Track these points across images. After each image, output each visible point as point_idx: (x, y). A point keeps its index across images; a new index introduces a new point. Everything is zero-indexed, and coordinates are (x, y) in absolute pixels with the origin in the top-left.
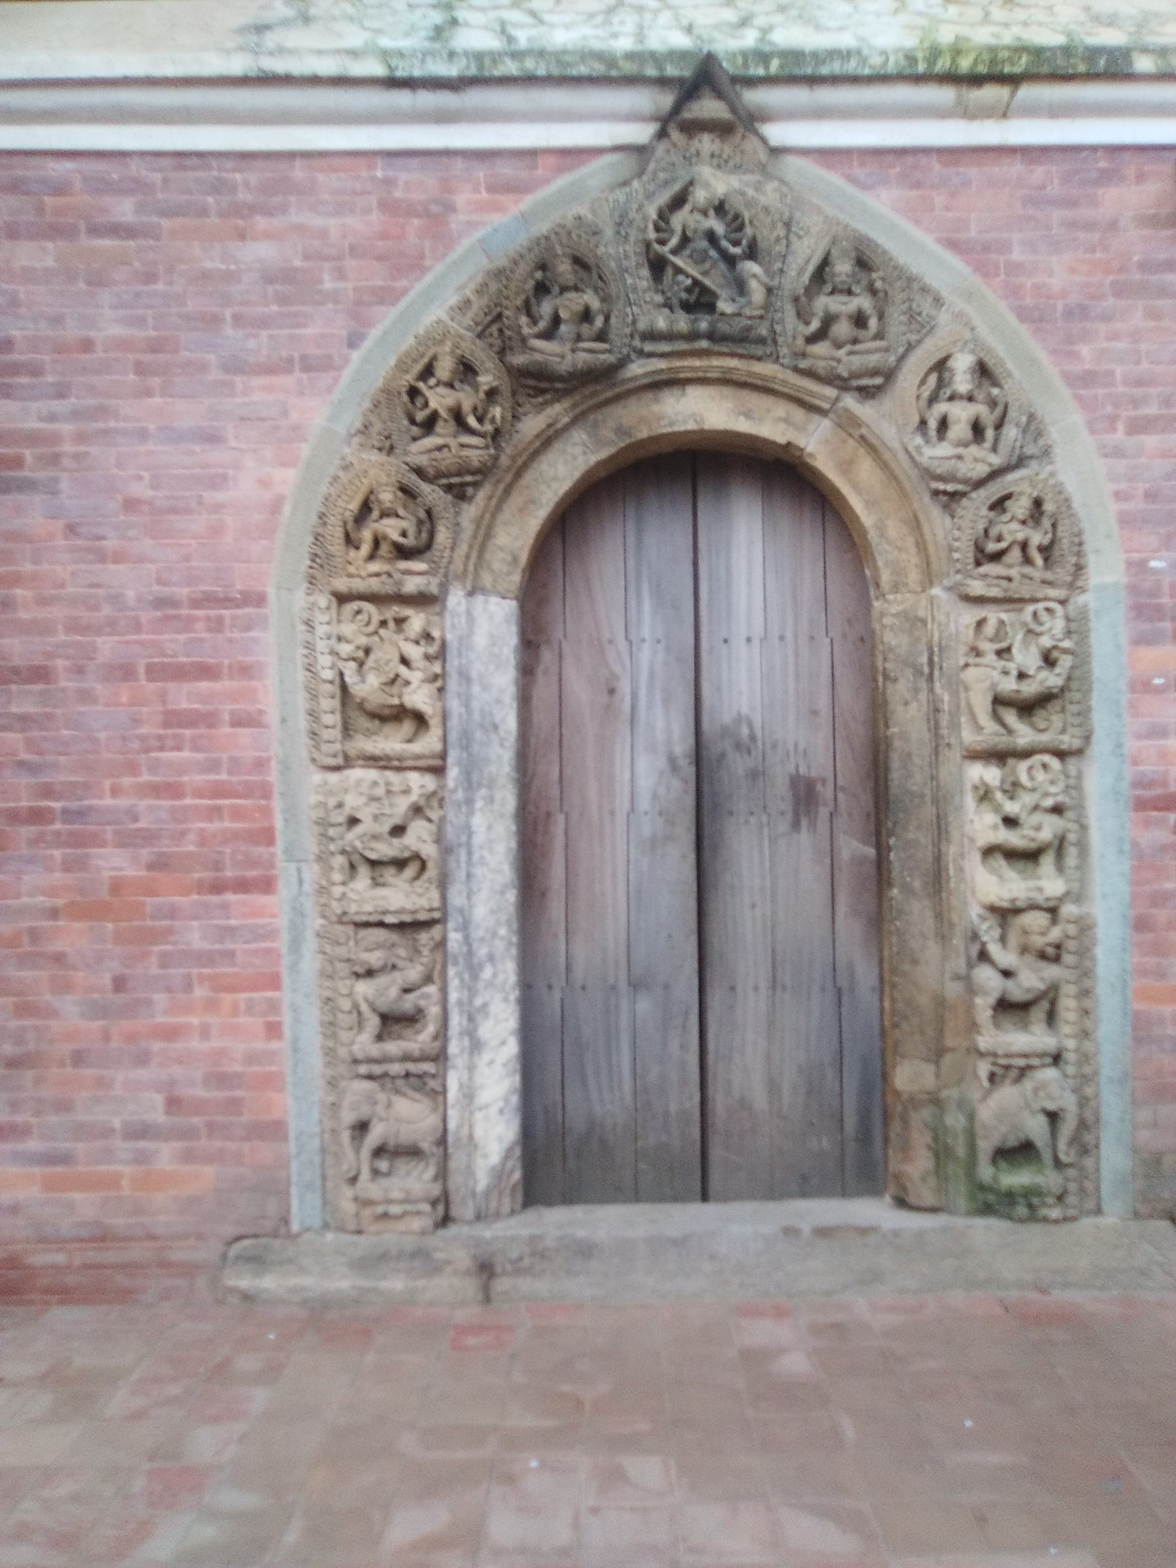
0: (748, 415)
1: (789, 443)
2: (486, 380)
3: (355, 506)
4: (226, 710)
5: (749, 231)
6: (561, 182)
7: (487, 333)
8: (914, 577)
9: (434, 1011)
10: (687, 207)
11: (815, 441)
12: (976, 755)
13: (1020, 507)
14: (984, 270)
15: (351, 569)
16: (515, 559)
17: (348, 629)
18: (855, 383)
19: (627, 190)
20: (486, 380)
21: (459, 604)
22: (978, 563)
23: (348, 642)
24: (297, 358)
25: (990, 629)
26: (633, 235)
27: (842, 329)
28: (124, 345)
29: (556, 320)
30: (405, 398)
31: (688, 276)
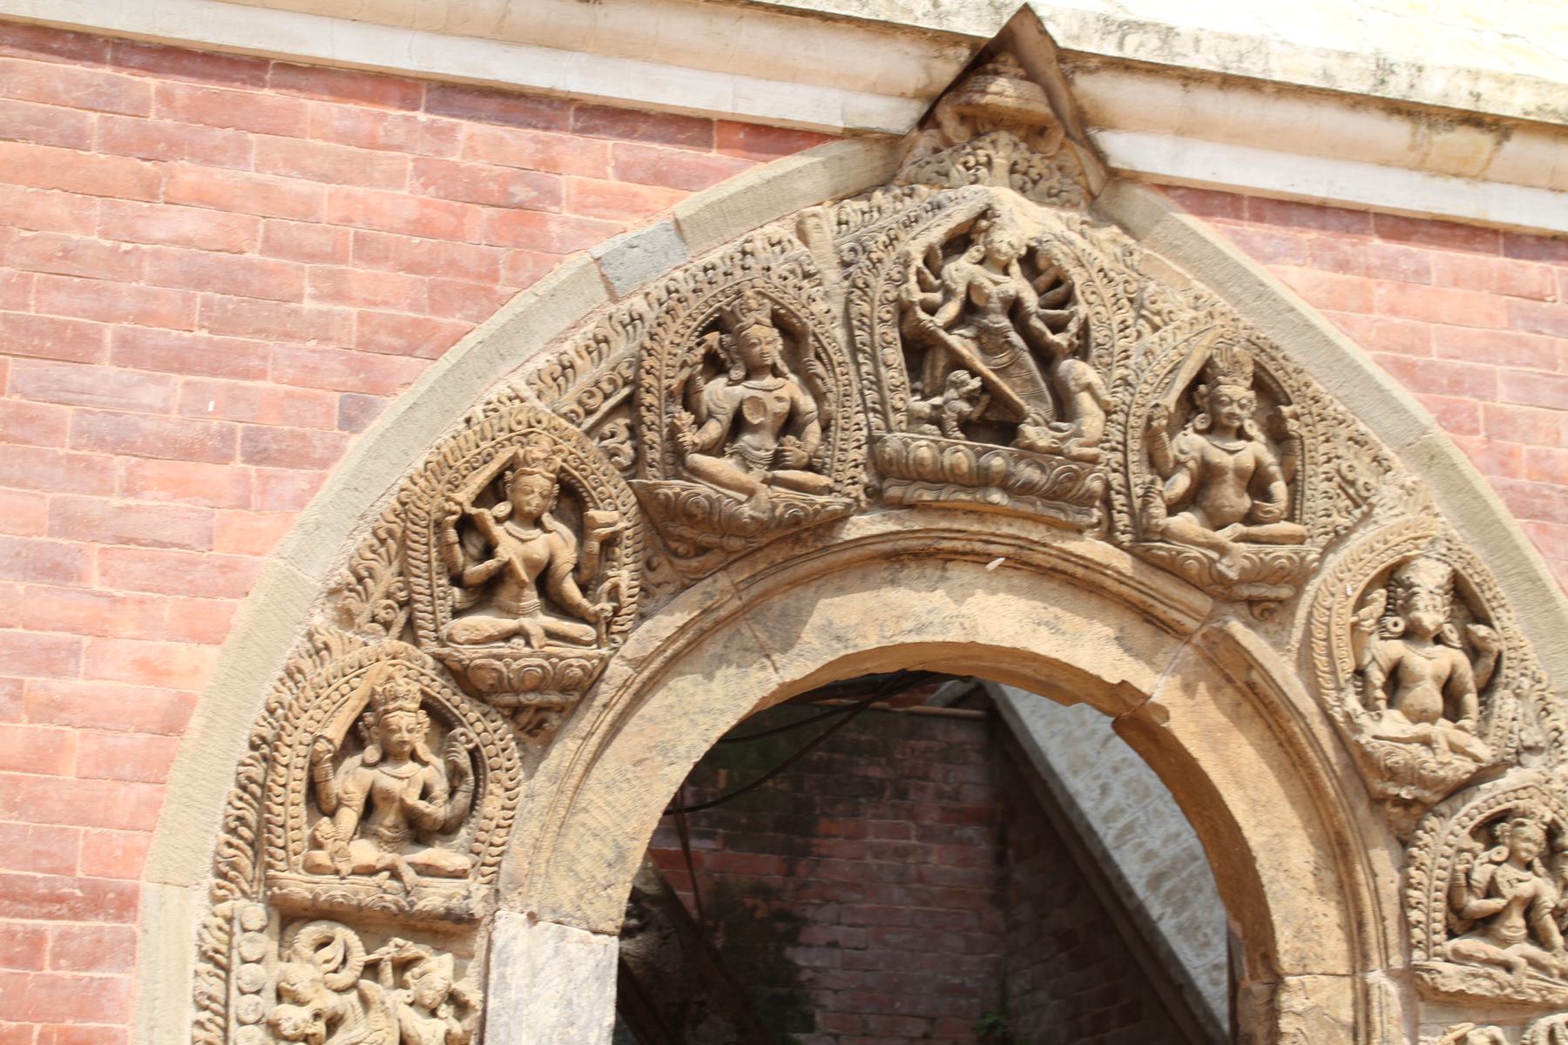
0: (1054, 629)
1: (1123, 682)
3: (337, 731)
5: (1082, 310)
7: (607, 428)
8: (1335, 946)
10: (974, 252)
15: (321, 857)
16: (622, 856)
18: (1246, 591)
19: (864, 205)
21: (514, 938)
22: (1451, 934)
23: (298, 1002)
24: (239, 435)
26: (879, 286)
29: (738, 425)
30: (452, 535)
31: (974, 373)
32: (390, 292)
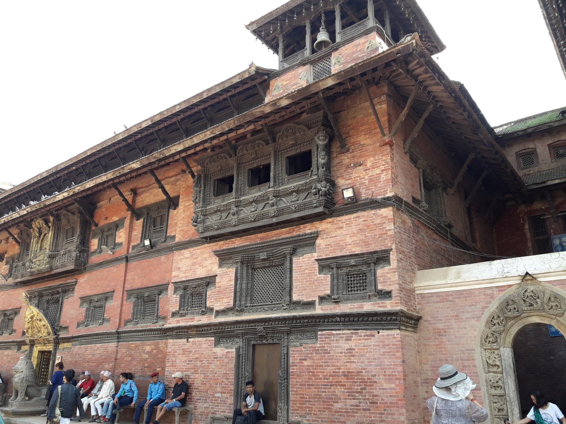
2: (501, 318)
4: (471, 365)
6: (509, 289)
9: (505, 408)
11: (553, 323)
17: (487, 354)
20: (501, 318)
27: (554, 307)
28: (453, 316)
32: (483, 304)
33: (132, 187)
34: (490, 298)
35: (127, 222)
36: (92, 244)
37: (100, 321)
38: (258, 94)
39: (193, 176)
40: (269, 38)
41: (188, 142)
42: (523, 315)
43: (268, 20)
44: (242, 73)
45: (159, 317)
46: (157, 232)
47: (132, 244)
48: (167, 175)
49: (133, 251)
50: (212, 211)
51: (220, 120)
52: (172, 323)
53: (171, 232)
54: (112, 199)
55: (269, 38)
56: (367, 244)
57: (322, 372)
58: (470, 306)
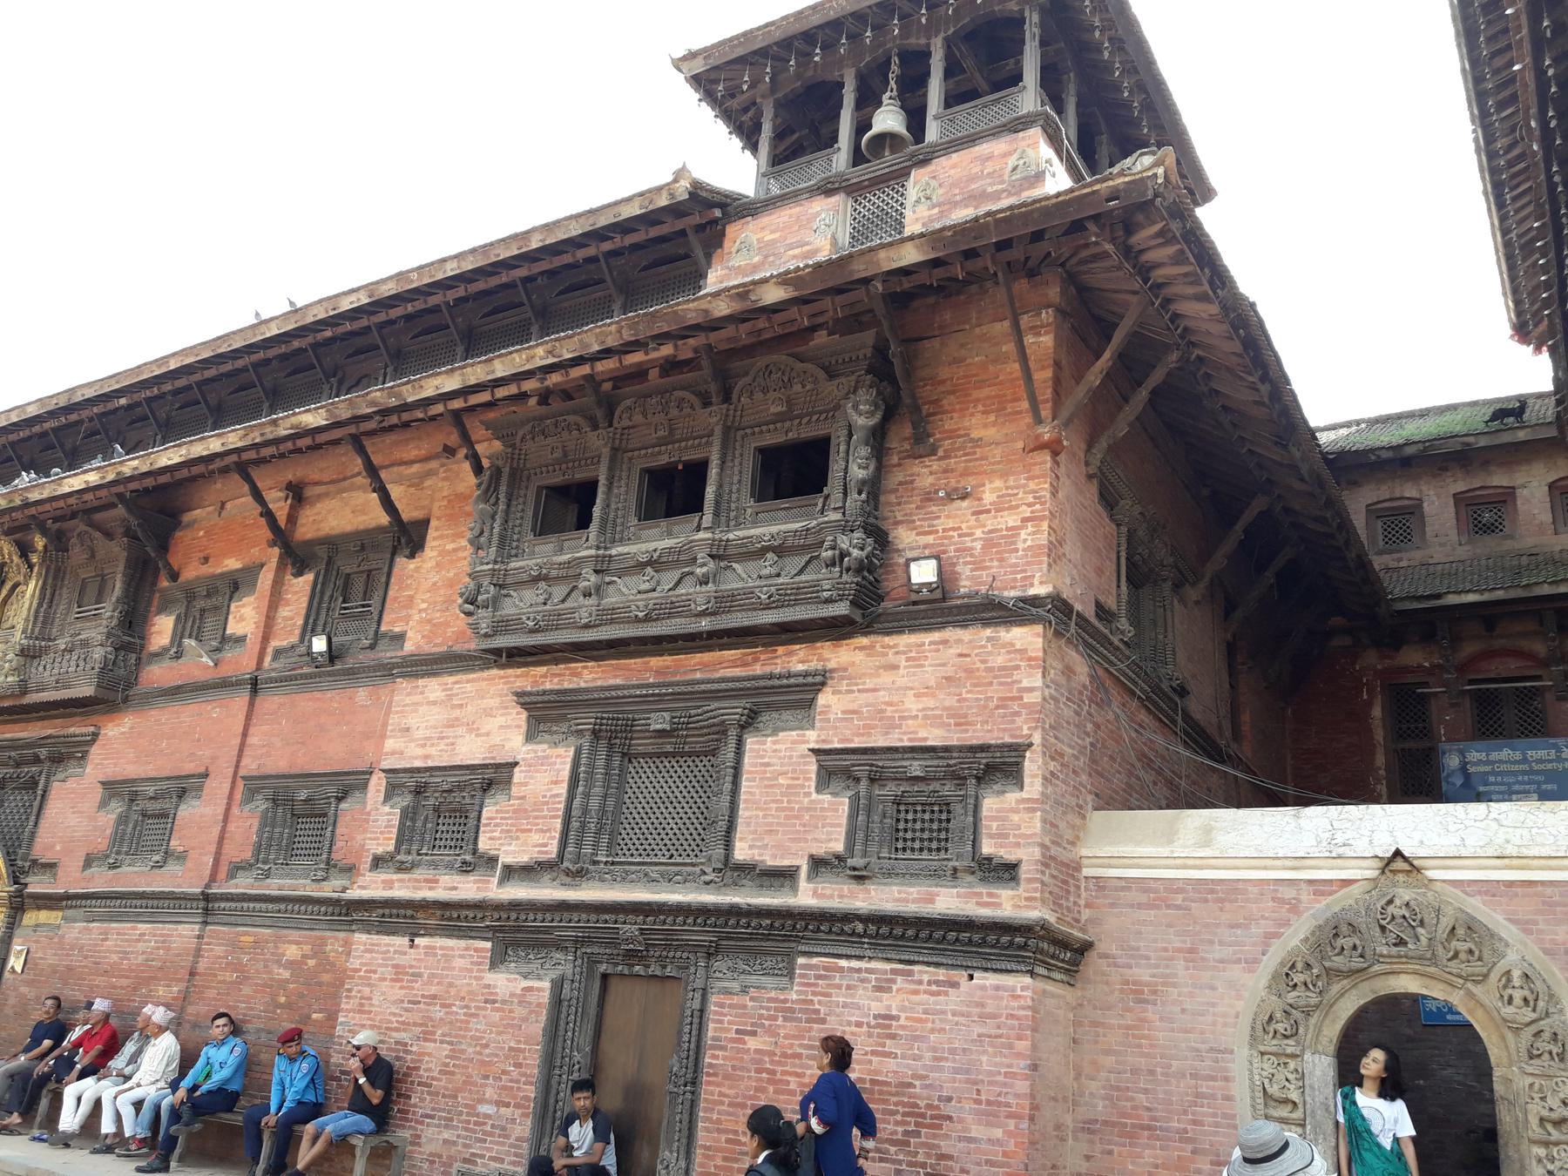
8: (1505, 1060)
11: (1456, 999)
12: (1535, 1142)
13: (1547, 1035)
14: (1527, 932)
20: (1315, 971)
25: (1536, 1087)
27: (1463, 956)
28: (1179, 950)
33: (290, 477)
34: (1289, 911)
35: (266, 579)
36: (154, 629)
37: (156, 858)
38: (687, 256)
39: (478, 469)
40: (734, 104)
41: (476, 372)
42: (1376, 968)
43: (740, 52)
44: (650, 191)
45: (335, 866)
46: (353, 616)
47: (275, 643)
48: (398, 455)
49: (275, 665)
50: (525, 577)
51: (575, 319)
52: (371, 886)
53: (393, 622)
54: (228, 506)
55: (734, 104)
56: (962, 722)
57: (797, 1075)
58: (1232, 927)
